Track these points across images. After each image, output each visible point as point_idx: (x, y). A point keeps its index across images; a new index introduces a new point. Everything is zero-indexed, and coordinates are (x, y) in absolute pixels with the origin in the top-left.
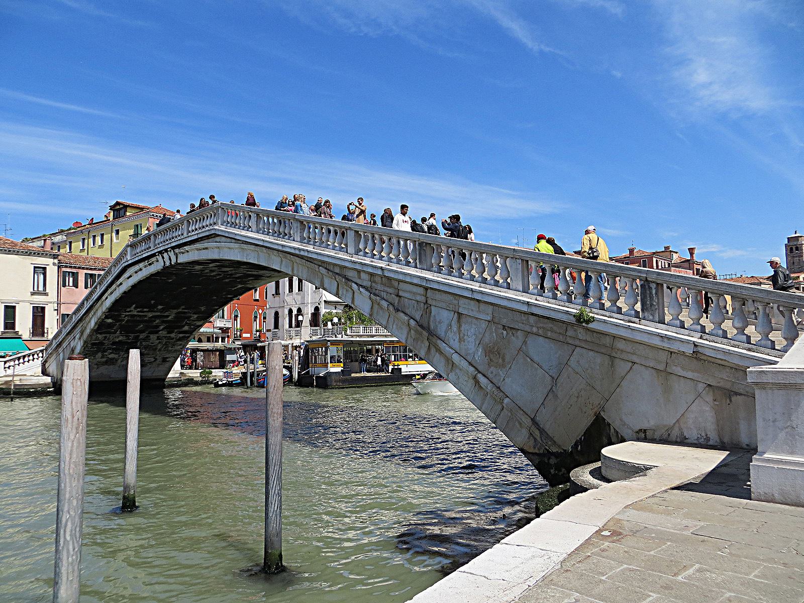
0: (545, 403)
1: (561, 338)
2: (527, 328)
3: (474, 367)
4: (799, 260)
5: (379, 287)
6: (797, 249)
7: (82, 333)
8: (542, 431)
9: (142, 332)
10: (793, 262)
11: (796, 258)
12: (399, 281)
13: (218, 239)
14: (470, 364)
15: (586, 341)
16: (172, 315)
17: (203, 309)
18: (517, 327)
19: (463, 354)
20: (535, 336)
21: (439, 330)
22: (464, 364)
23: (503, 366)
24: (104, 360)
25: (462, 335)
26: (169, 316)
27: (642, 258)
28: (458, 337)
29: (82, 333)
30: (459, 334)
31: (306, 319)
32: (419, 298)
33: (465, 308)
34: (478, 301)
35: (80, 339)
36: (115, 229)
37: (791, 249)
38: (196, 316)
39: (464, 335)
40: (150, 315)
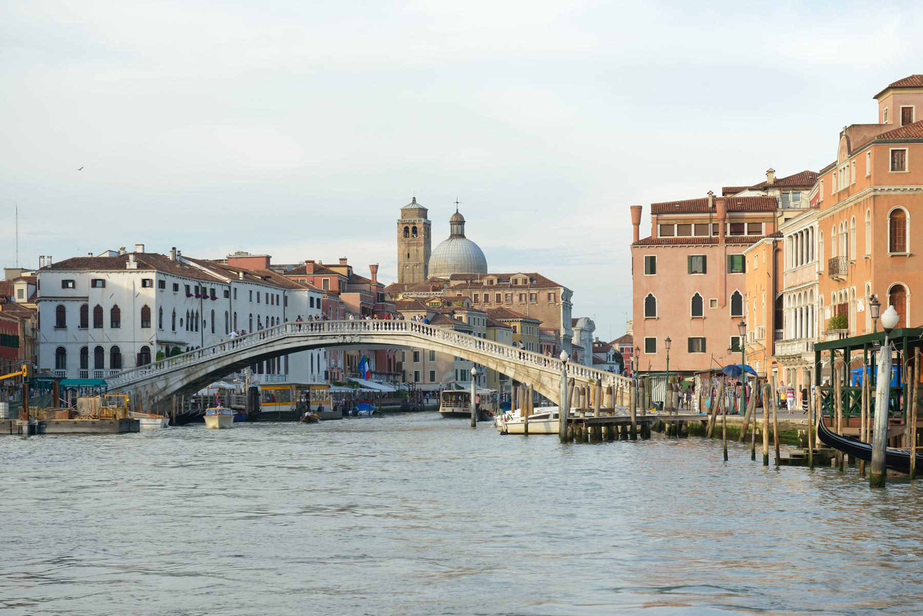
4: (417, 251)
6: (415, 230)
10: (409, 254)
11: (412, 248)
29: (188, 376)
33: (554, 377)
37: (406, 229)
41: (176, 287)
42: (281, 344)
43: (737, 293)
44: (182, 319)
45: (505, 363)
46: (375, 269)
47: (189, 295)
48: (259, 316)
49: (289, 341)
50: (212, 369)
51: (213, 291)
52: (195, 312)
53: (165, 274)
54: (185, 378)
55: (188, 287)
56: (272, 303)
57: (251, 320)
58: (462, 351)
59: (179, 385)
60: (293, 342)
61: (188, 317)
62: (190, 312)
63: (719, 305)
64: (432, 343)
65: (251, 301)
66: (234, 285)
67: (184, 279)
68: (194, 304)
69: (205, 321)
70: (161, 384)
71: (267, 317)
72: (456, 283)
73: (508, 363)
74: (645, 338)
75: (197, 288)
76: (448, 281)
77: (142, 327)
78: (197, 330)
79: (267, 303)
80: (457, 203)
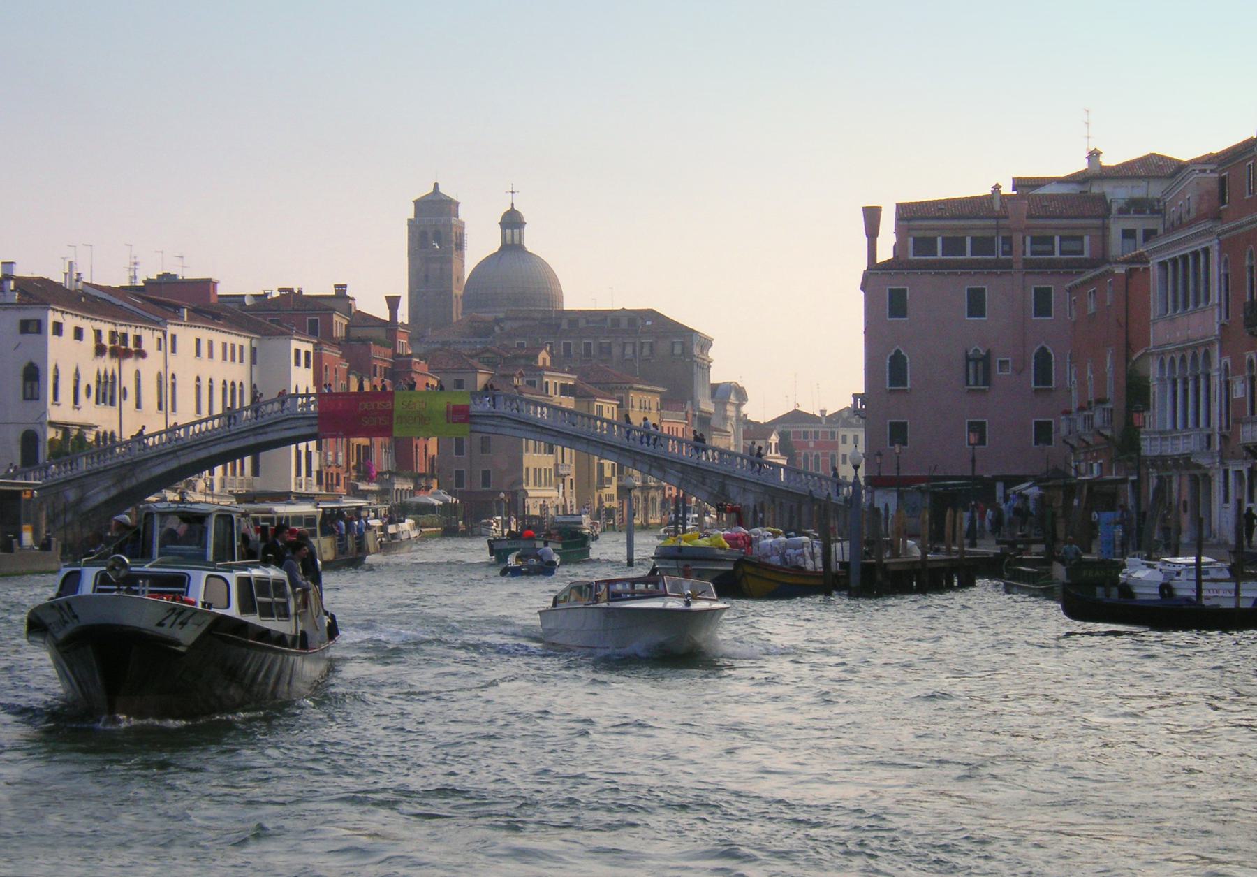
4: (441, 269)
6: (438, 237)
10: (427, 276)
27: (309, 315)
35: (107, 489)
41: (79, 334)
42: (277, 431)
43: (1043, 349)
44: (89, 387)
47: (100, 350)
48: (211, 381)
49: (293, 425)
50: (159, 470)
51: (138, 340)
52: (110, 374)
53: (63, 312)
54: (114, 485)
55: (98, 333)
56: (233, 359)
57: (198, 388)
59: (103, 497)
60: (300, 427)
61: (99, 382)
62: (102, 374)
63: (1013, 369)
64: (539, 430)
65: (198, 354)
66: (171, 330)
67: (92, 319)
68: (108, 364)
69: (125, 389)
70: (72, 495)
71: (225, 383)
72: (516, 324)
74: (888, 421)
75: (113, 334)
76: (502, 320)
77: (25, 398)
78: (112, 403)
79: (225, 358)
80: (512, 192)
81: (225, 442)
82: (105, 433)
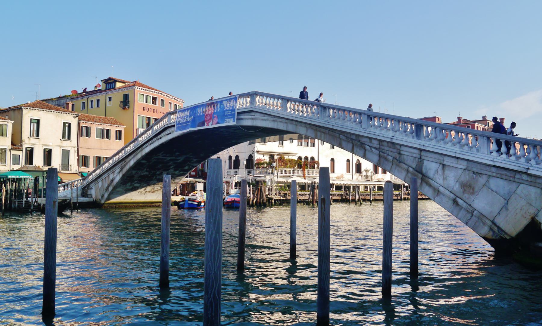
0: (500, 213)
1: (512, 179)
2: (490, 174)
3: (453, 194)
5: (386, 148)
7: (121, 169)
8: (499, 228)
9: (159, 169)
12: (401, 145)
13: (253, 114)
14: (451, 192)
15: (527, 181)
16: (181, 159)
17: (202, 155)
18: (483, 173)
19: (446, 186)
20: (494, 178)
21: (429, 173)
22: (447, 193)
23: (473, 193)
24: (131, 187)
25: (445, 176)
26: (180, 159)
27: (467, 125)
28: (442, 178)
29: (121, 169)
30: (443, 176)
31: (243, 163)
32: (415, 155)
33: (447, 161)
34: (458, 158)
35: (119, 173)
36: (108, 96)
38: (195, 160)
39: (447, 176)
40: (169, 158)
45: (364, 140)
46: (513, 125)
58: (307, 126)
59: (118, 179)
73: (368, 140)
81: (149, 145)
82: (306, 158)
